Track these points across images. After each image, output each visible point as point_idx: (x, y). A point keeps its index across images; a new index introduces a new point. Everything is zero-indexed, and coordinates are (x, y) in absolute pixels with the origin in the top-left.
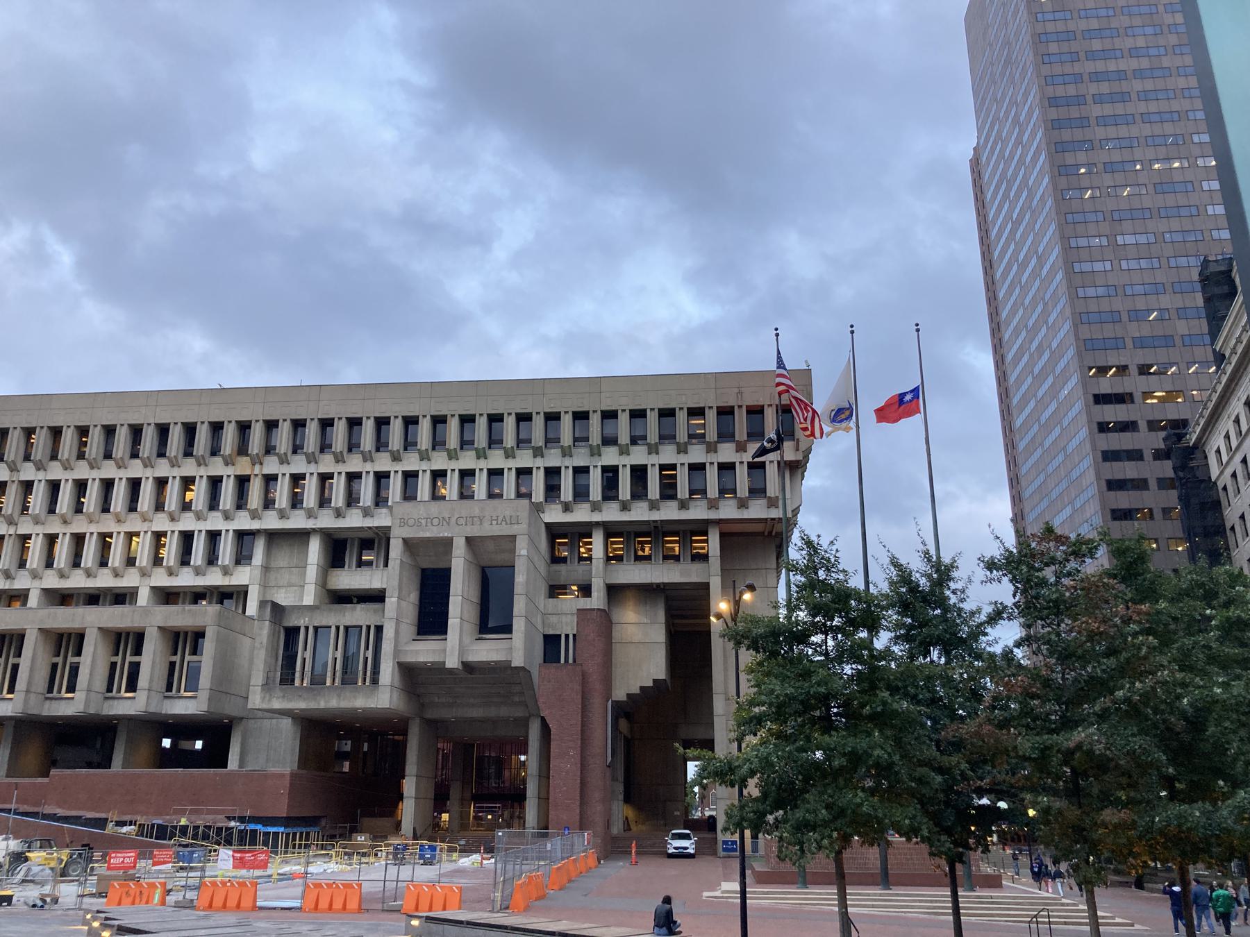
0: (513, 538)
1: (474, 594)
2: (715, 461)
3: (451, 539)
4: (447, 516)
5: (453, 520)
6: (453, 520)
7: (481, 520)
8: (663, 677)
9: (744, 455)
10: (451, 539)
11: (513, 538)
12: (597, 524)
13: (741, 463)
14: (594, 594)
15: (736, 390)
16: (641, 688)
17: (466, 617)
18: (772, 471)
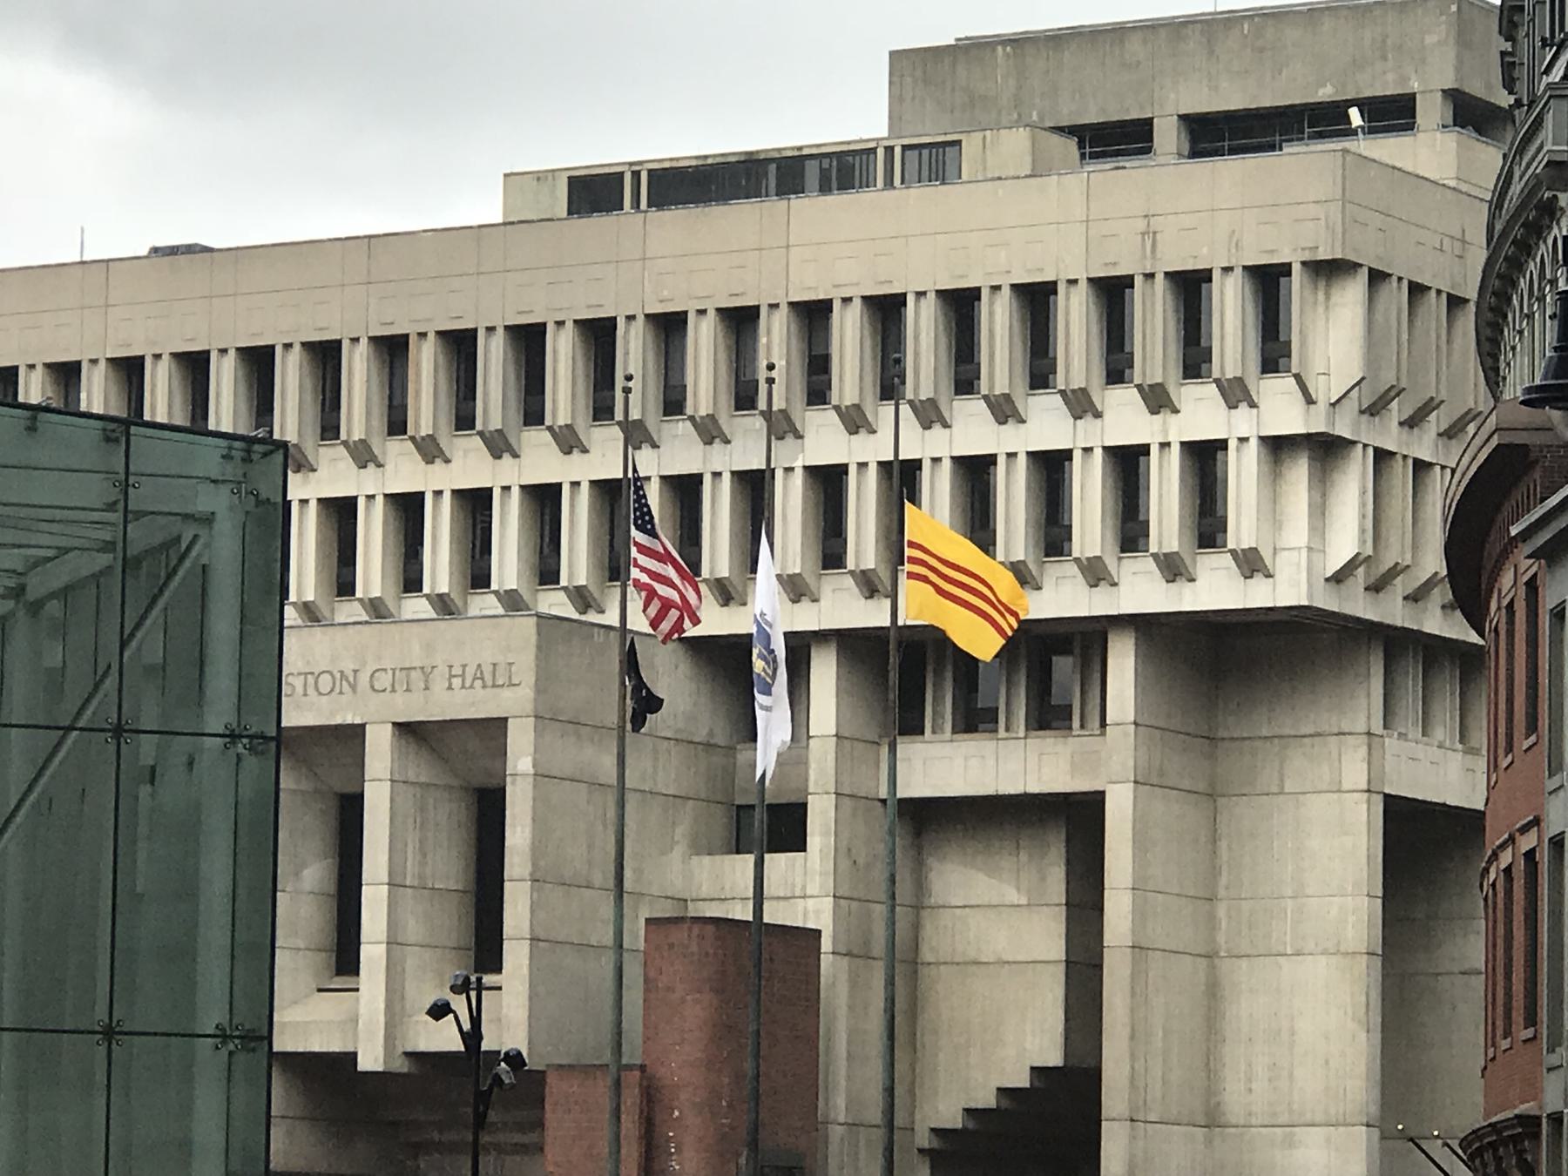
0: (497, 726)
1: (449, 867)
2: (1097, 443)
3: (363, 726)
4: (349, 666)
5: (364, 678)
6: (364, 678)
7: (427, 673)
8: (1054, 1059)
9: (1173, 419)
10: (363, 726)
11: (497, 726)
12: (822, 636)
13: (1165, 445)
14: (814, 840)
15: (1141, 225)
16: (1002, 1091)
17: (413, 929)
18: (1243, 473)
